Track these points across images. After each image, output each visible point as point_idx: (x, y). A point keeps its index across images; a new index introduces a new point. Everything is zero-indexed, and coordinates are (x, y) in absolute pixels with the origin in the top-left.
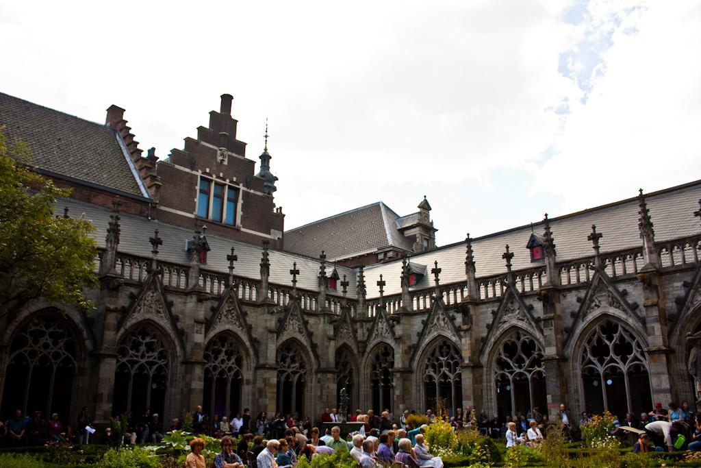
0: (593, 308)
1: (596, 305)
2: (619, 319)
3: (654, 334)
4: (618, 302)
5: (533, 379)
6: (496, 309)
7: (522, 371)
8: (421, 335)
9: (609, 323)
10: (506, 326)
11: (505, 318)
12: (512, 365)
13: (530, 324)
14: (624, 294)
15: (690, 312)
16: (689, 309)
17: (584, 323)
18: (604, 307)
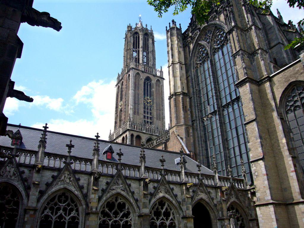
0: (159, 193)
1: (161, 192)
2: (168, 200)
3: (189, 210)
4: (169, 192)
5: (123, 225)
6: (109, 181)
7: (117, 219)
8: (49, 185)
9: (162, 201)
10: (114, 192)
11: (114, 187)
12: (112, 215)
13: (128, 194)
14: (172, 189)
15: (194, 202)
16: (193, 201)
17: (155, 199)
18: (118, 189)
